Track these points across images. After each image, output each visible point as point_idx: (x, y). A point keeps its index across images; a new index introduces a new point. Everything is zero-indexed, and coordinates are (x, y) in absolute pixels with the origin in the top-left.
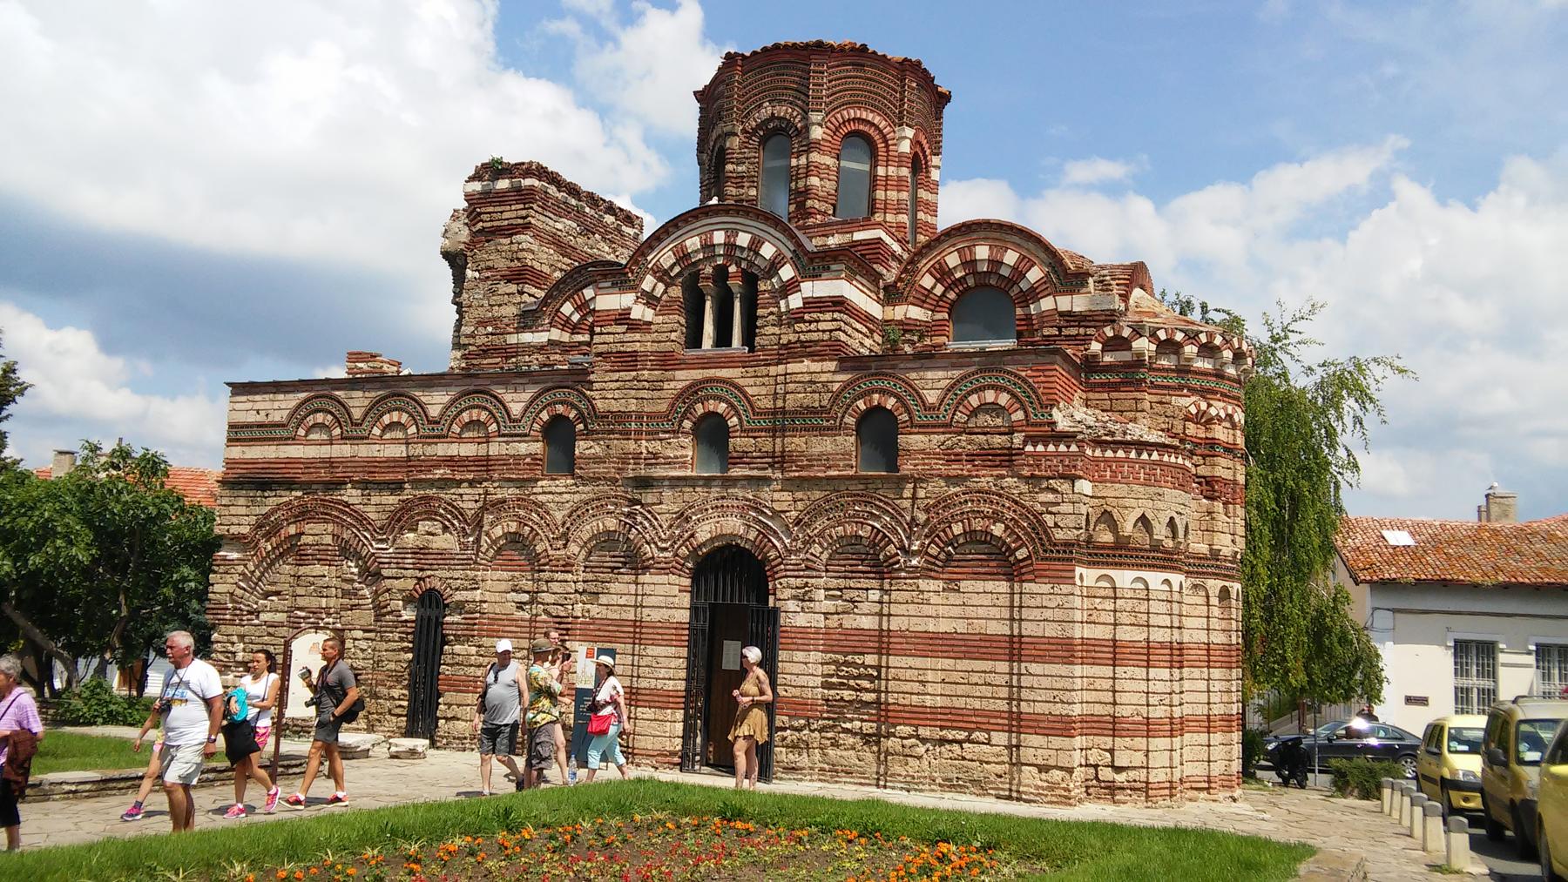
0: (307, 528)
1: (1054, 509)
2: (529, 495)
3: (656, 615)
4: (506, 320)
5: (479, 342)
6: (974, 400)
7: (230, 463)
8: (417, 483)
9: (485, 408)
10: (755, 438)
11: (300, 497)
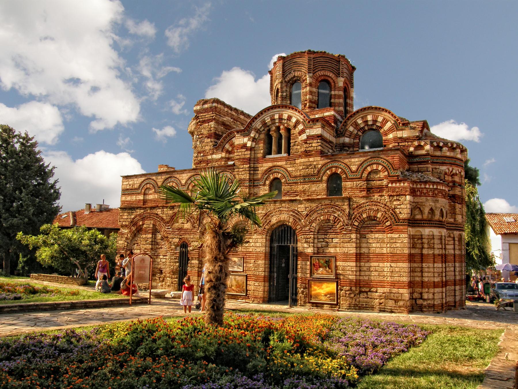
3: (258, 250)
4: (207, 151)
5: (199, 159)
6: (369, 169)
7: (123, 202)
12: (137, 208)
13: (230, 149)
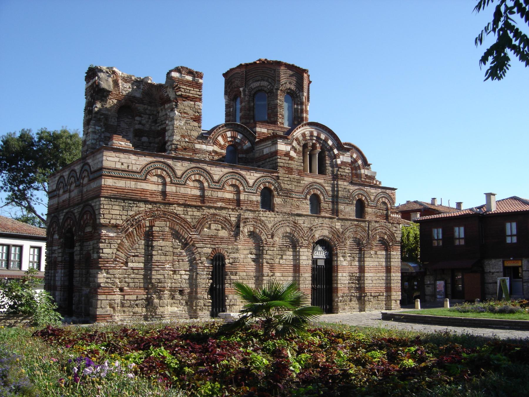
0: (157, 223)
1: (396, 232)
2: (257, 217)
8: (210, 208)
9: (238, 180)
10: (328, 204)
11: (150, 209)
12: (140, 201)
13: (222, 143)
